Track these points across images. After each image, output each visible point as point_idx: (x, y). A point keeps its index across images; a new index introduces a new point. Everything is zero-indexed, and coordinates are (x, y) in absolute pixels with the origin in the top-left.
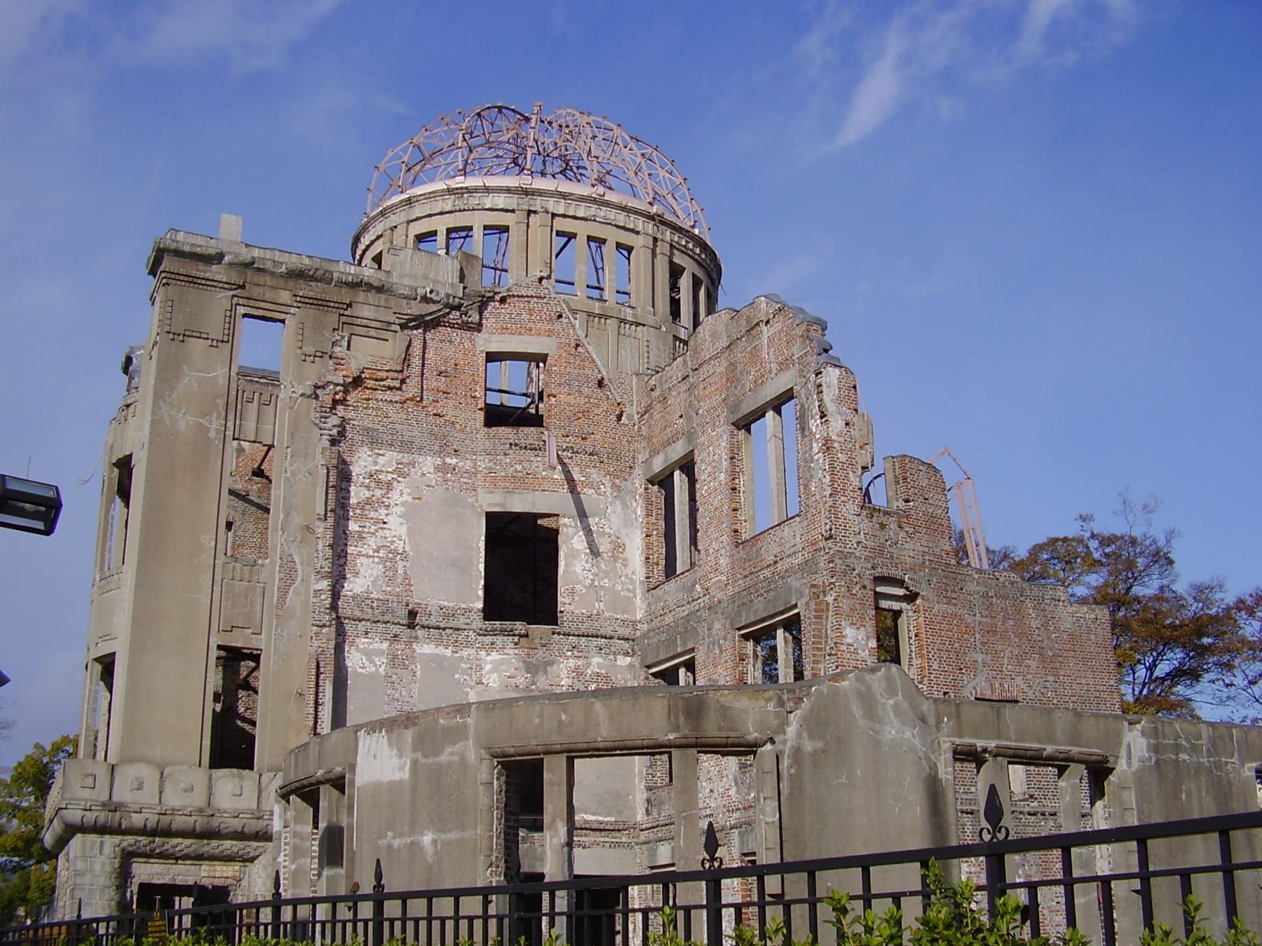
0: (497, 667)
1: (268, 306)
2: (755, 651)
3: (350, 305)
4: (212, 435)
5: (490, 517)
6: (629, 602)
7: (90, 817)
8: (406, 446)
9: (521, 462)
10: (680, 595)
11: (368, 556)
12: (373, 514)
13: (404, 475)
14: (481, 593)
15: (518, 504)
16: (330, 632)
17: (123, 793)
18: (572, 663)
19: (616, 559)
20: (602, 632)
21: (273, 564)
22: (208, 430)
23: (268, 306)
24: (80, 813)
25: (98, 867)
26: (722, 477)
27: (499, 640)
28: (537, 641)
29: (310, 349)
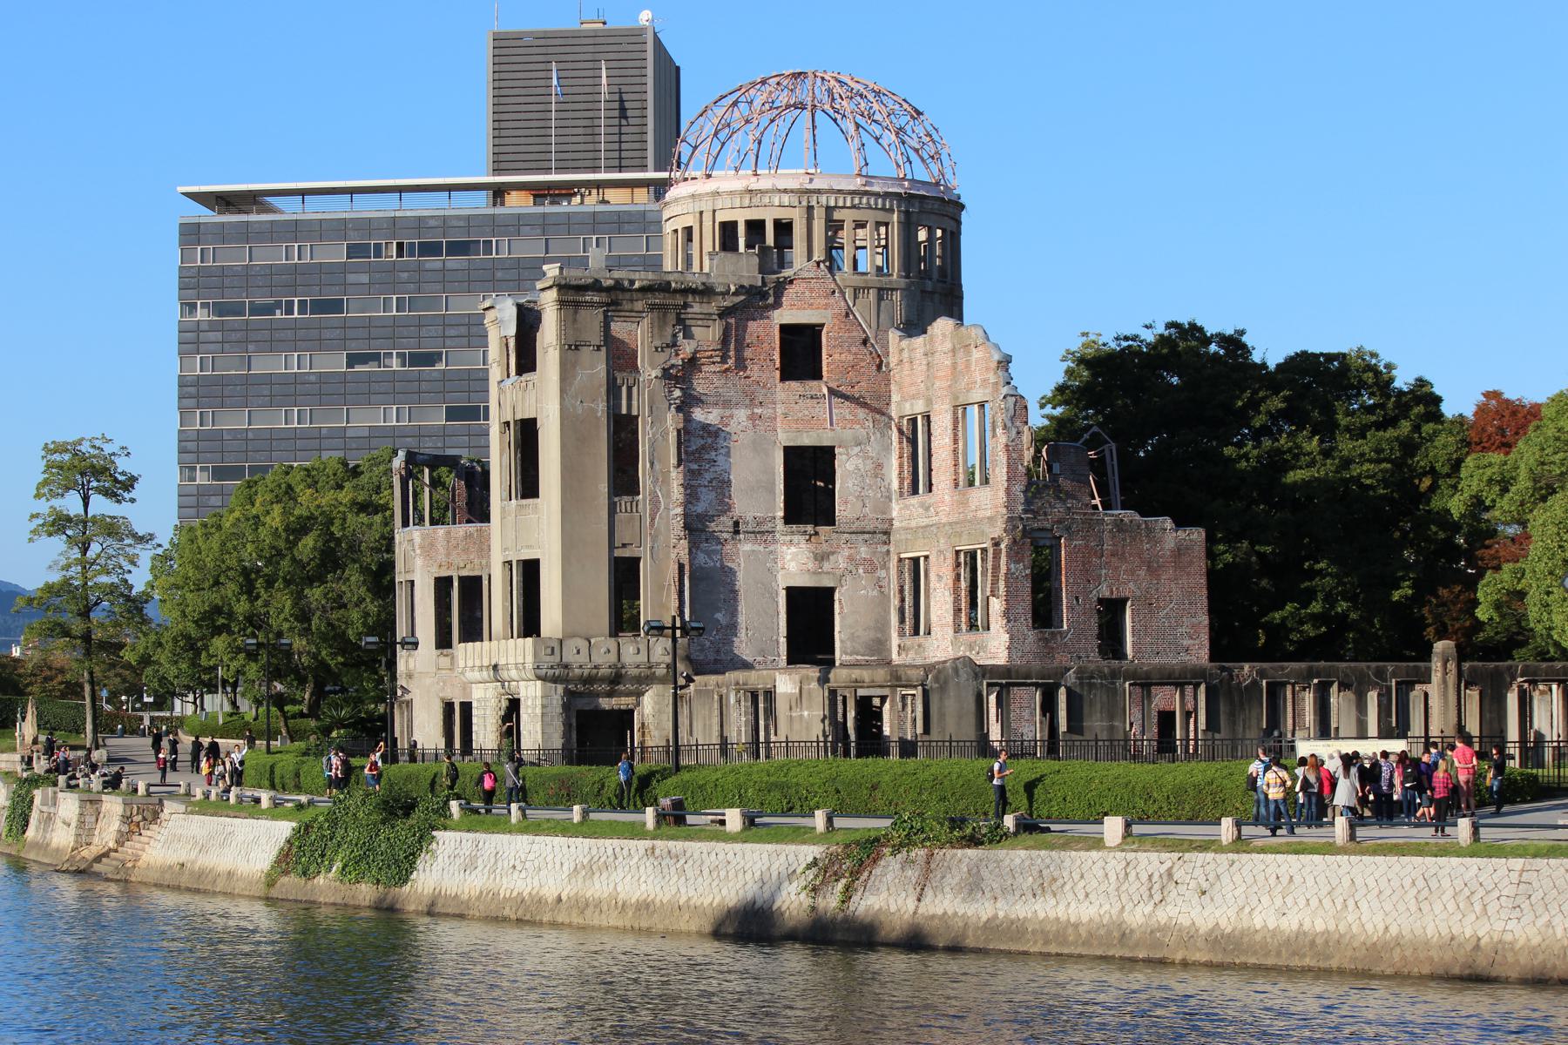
0: (795, 555)
1: (628, 314)
2: (965, 561)
3: (686, 306)
4: (599, 414)
5: (788, 451)
6: (886, 509)
7: (551, 672)
8: (727, 404)
10: (921, 510)
11: (705, 486)
12: (706, 457)
14: (782, 505)
15: (806, 441)
16: (684, 543)
17: (569, 656)
18: (846, 553)
19: (876, 477)
20: (868, 529)
21: (644, 499)
22: (597, 411)
23: (628, 314)
24: (544, 671)
25: (555, 702)
26: (947, 440)
27: (796, 538)
29: (658, 343)
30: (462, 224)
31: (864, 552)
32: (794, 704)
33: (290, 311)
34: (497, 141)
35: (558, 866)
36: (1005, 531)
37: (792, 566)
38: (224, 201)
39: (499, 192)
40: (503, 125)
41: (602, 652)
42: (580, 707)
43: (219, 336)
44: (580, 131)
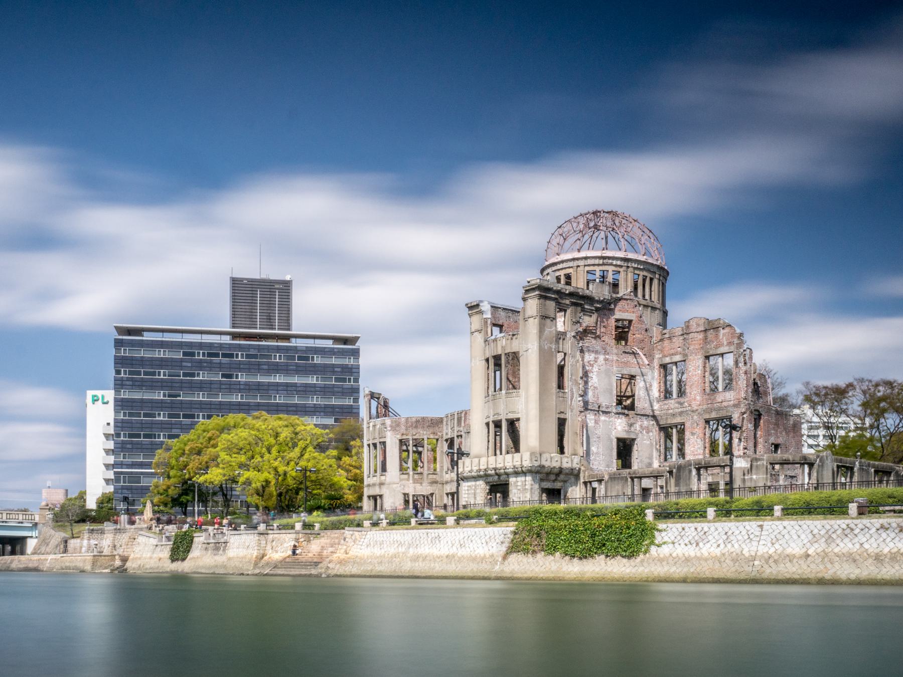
7: (537, 468)
9: (625, 357)
13: (596, 362)
17: (544, 463)
18: (640, 423)
22: (552, 349)
27: (621, 416)
28: (631, 416)
30: (227, 346)
31: (646, 423)
32: (746, 472)
33: (159, 375)
34: (234, 319)
35: (795, 537)
36: (747, 409)
37: (619, 428)
38: (130, 332)
39: (235, 336)
40: (236, 313)
41: (553, 460)
42: (542, 486)
43: (131, 383)
44: (265, 317)
